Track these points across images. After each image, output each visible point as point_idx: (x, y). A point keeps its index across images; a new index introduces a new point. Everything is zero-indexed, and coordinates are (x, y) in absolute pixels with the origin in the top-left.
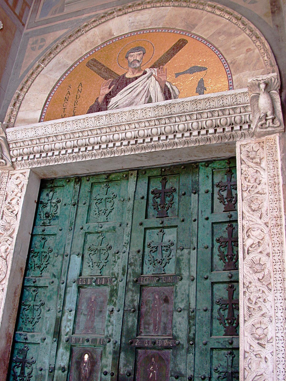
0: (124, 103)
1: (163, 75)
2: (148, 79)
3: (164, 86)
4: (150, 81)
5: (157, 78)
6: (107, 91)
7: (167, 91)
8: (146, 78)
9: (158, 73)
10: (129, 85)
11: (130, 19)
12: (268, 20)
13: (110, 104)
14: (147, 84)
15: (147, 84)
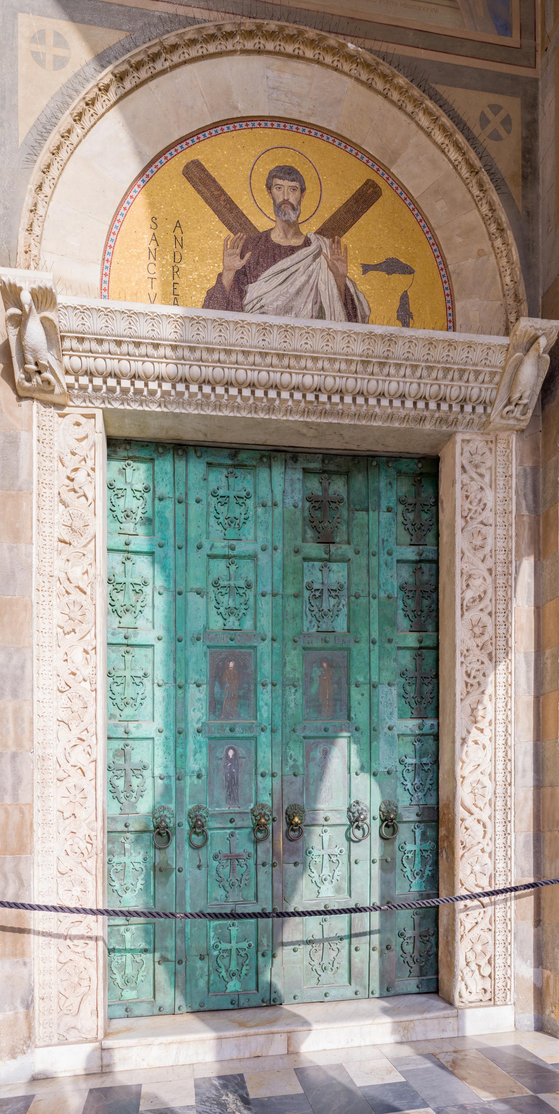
0: (275, 304)
1: (342, 260)
2: (314, 260)
3: (343, 288)
4: (318, 267)
5: (330, 263)
6: (238, 264)
7: (349, 301)
8: (310, 258)
9: (333, 253)
10: (280, 263)
11: (270, 73)
12: (515, 190)
13: (248, 298)
14: (313, 272)
15: (313, 272)
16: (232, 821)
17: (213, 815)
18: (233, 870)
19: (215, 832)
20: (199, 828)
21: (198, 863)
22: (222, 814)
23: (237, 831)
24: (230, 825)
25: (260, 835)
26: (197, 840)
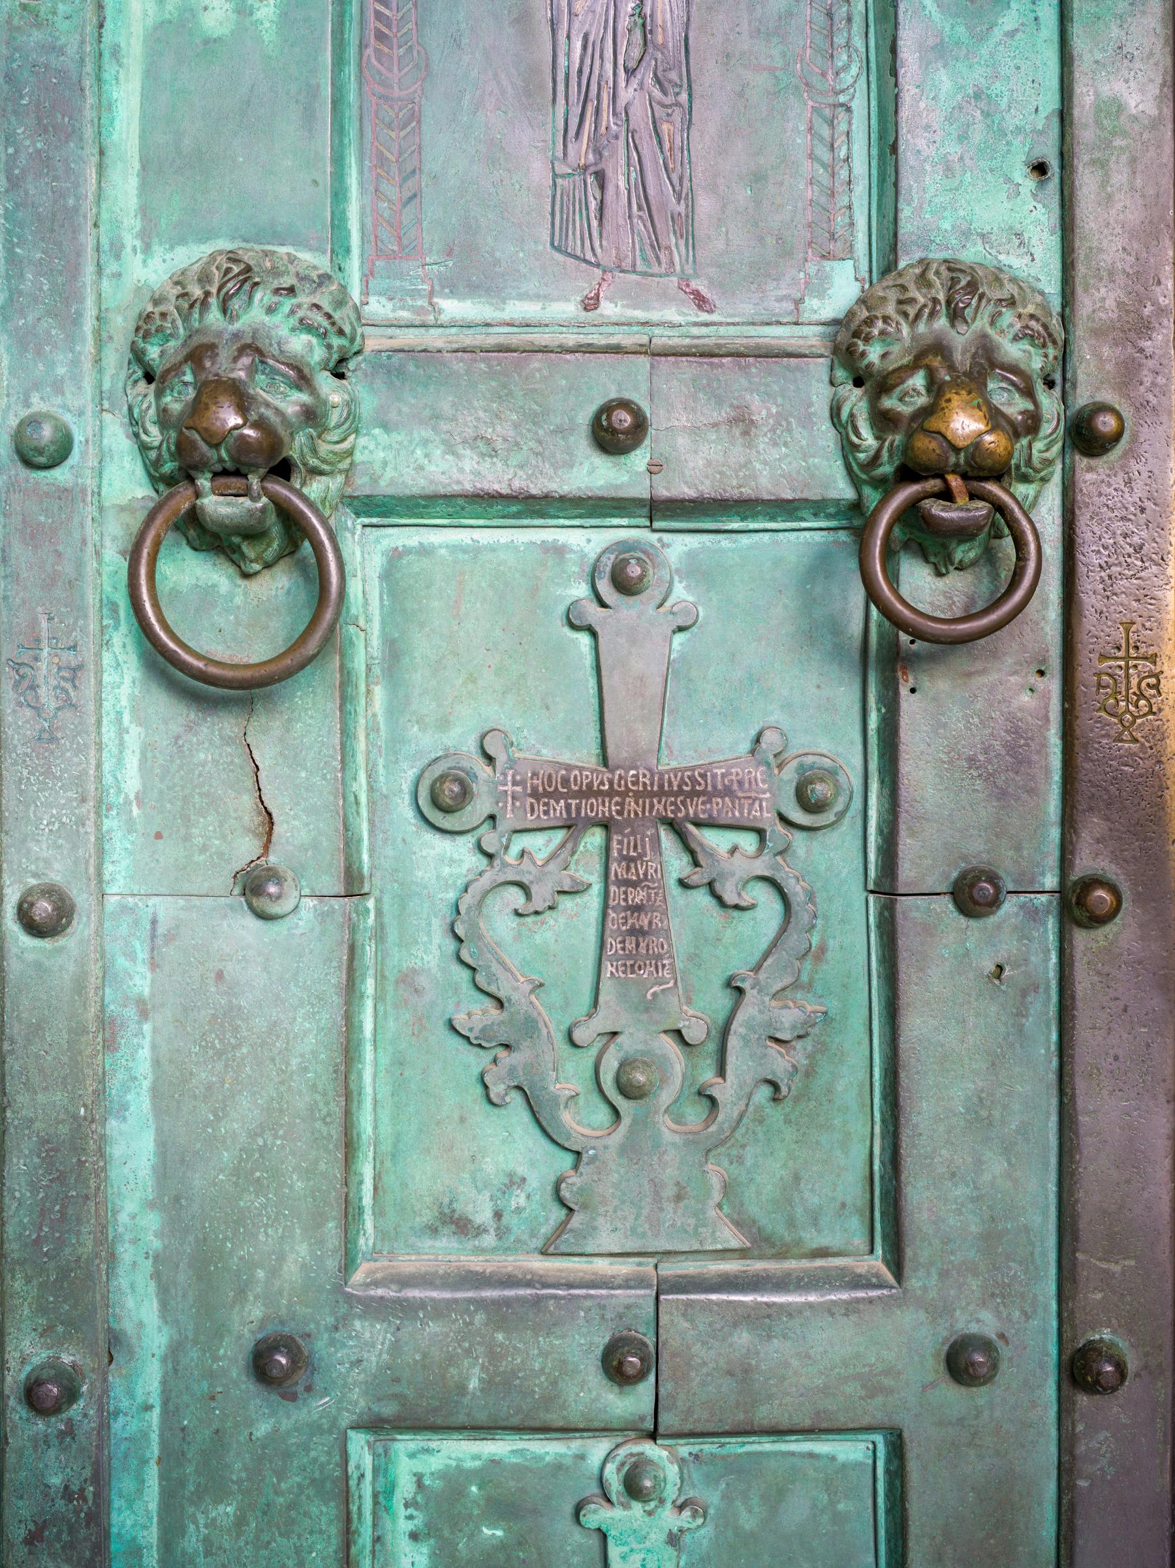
16: (614, 433)
17: (408, 366)
18: (632, 933)
19: (443, 538)
20: (231, 473)
21: (246, 849)
22: (510, 354)
23: (678, 546)
24: (596, 474)
25: (921, 587)
26: (228, 610)
